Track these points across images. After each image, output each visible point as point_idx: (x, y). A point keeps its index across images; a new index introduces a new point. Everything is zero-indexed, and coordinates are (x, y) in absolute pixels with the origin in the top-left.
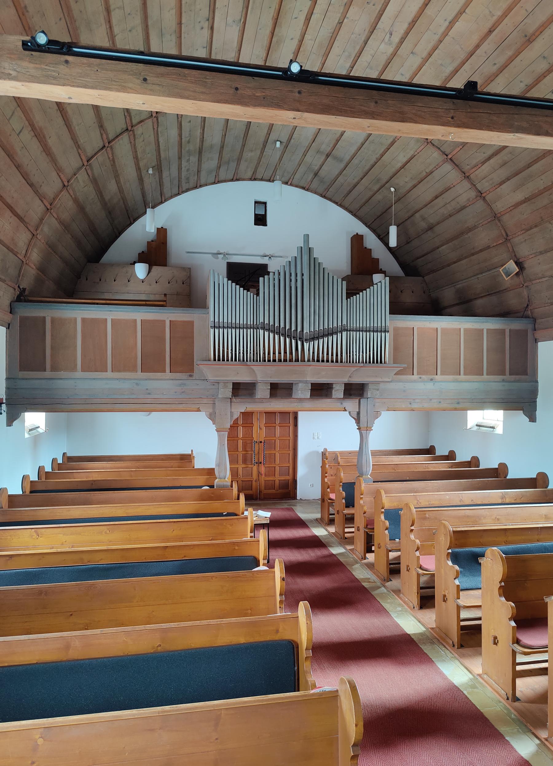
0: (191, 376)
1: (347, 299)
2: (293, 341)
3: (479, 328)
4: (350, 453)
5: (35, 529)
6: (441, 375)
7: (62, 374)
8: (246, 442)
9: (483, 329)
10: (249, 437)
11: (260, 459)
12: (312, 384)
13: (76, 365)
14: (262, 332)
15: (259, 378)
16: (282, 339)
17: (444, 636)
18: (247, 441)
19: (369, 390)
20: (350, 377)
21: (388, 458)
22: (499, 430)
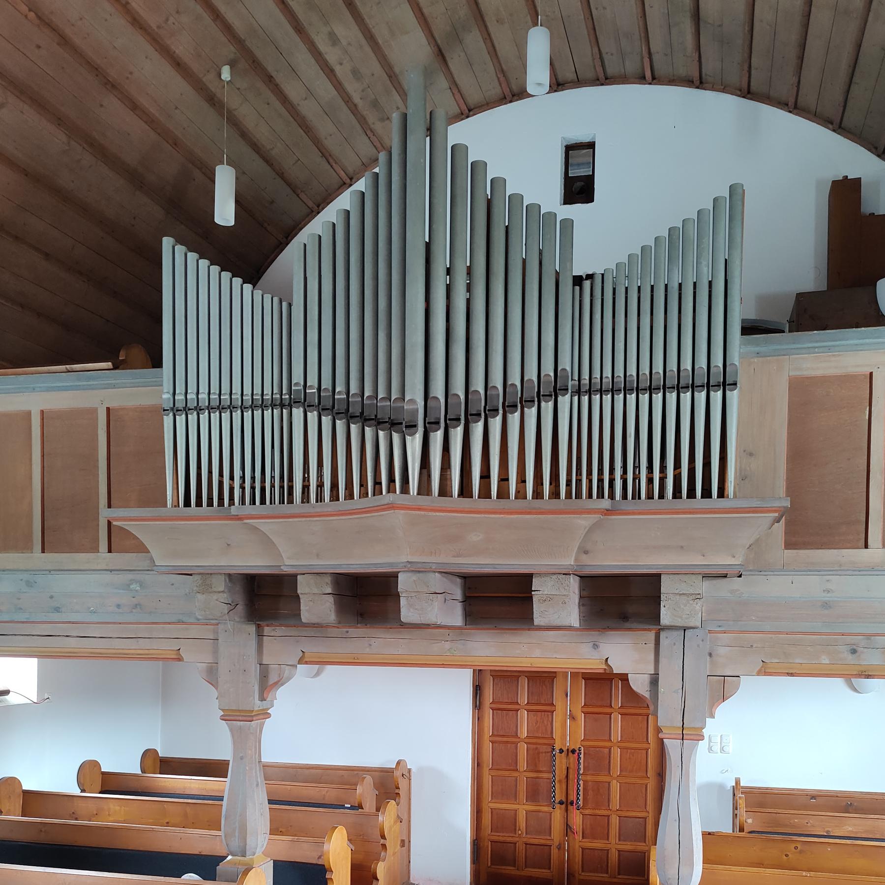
8: (537, 748)
11: (570, 792)
18: (539, 746)
20: (586, 552)
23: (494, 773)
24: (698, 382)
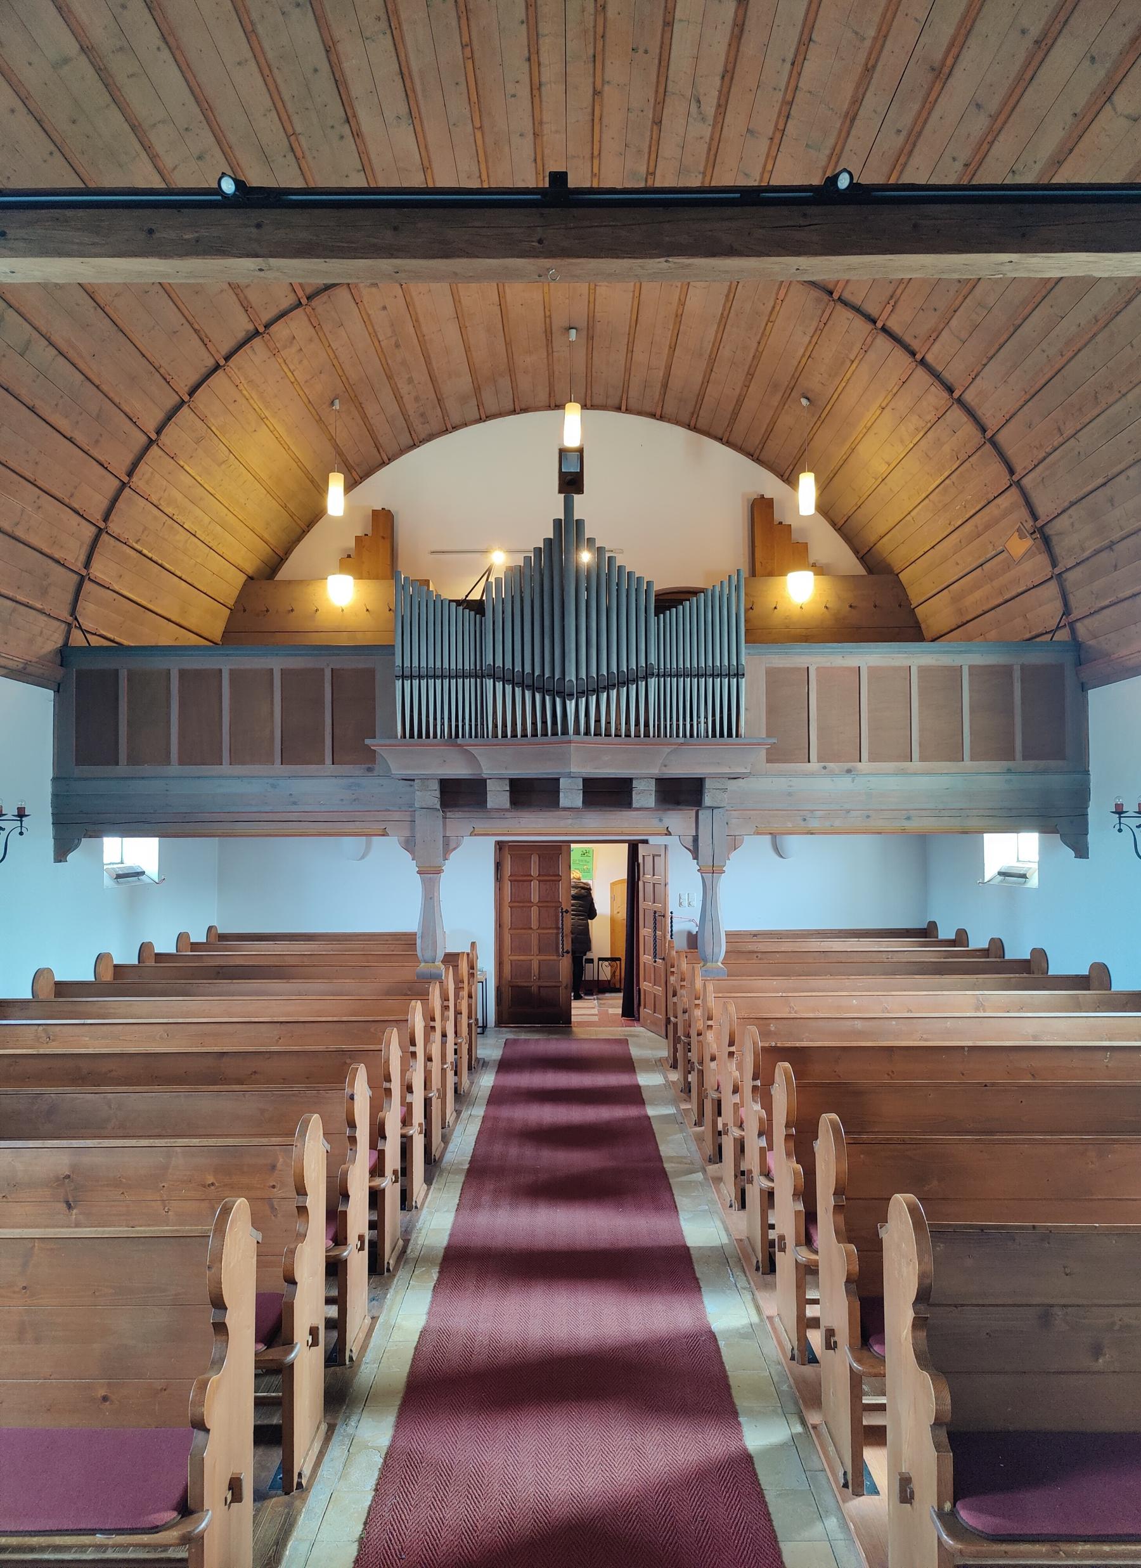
0: (369, 770)
1: (657, 615)
2: (547, 698)
3: (954, 664)
4: (755, 935)
5: (44, 1027)
6: (869, 761)
7: (147, 769)
9: (961, 666)
10: (553, 902)
12: (585, 780)
13: (168, 753)
14: (489, 683)
15: (486, 771)
16: (528, 694)
17: (750, 1250)
19: (706, 791)
20: (665, 766)
21: (822, 943)
22: (1034, 882)
23: (512, 932)
24: (723, 673)
